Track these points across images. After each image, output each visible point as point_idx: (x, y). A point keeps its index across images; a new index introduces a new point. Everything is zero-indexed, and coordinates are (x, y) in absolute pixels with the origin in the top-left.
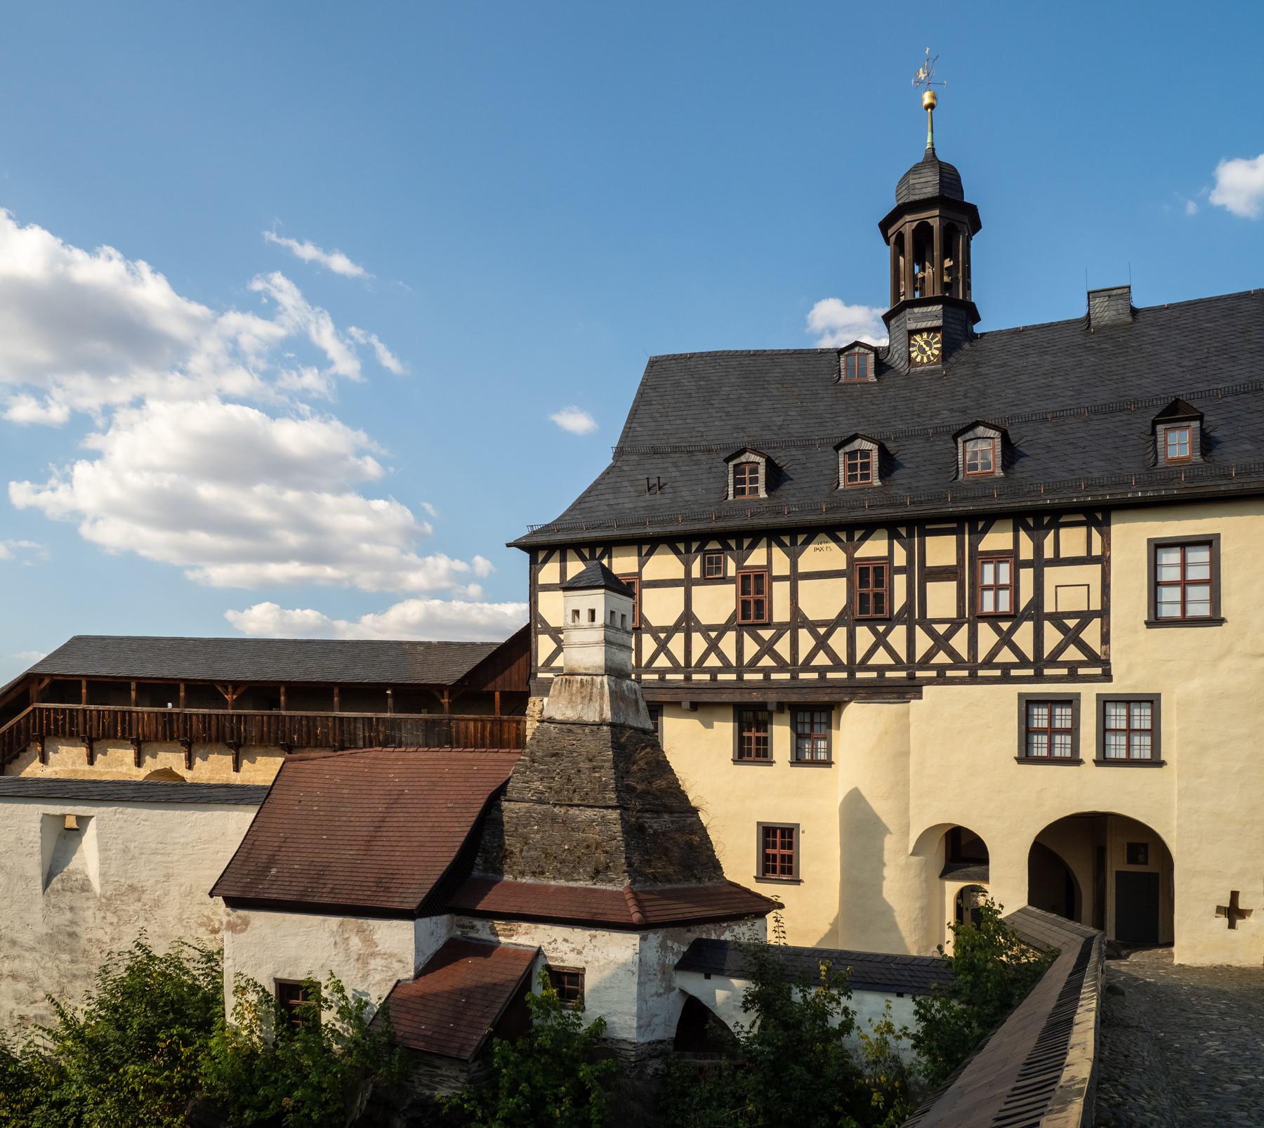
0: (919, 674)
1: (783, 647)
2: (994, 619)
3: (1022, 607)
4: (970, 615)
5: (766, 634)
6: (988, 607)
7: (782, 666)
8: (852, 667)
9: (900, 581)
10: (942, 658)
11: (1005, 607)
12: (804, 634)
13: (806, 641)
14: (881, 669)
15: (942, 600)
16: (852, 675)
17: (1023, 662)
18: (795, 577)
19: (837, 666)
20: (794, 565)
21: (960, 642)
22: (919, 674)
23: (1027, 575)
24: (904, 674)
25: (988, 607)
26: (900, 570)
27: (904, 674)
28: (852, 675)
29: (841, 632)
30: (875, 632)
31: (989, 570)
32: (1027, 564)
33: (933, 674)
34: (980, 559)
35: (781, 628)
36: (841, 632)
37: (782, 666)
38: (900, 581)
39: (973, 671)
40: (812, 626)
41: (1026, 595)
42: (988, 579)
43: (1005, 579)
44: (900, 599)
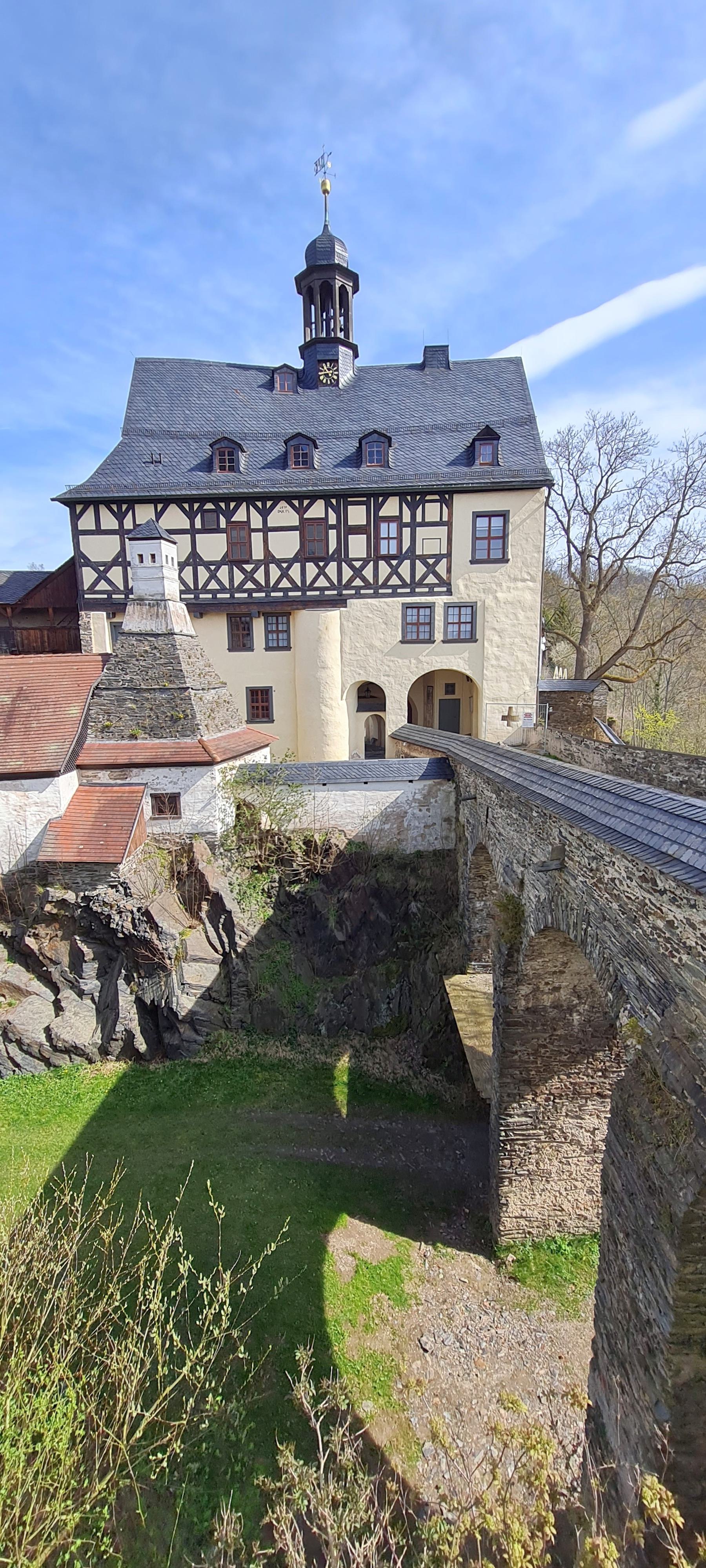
0: (344, 592)
1: (260, 576)
2: (388, 558)
3: (404, 551)
4: (375, 556)
5: (248, 567)
6: (383, 551)
8: (304, 588)
9: (333, 534)
10: (358, 582)
11: (393, 551)
12: (273, 567)
13: (275, 572)
15: (358, 546)
16: (304, 594)
17: (404, 585)
18: (266, 530)
19: (295, 588)
20: (265, 522)
21: (368, 572)
22: (344, 592)
23: (406, 531)
24: (335, 592)
25: (383, 551)
26: (332, 527)
27: (335, 592)
28: (304, 594)
29: (297, 566)
30: (318, 566)
31: (384, 526)
32: (407, 525)
33: (353, 592)
34: (379, 520)
36: (297, 566)
37: (259, 589)
38: (333, 534)
39: (376, 589)
40: (278, 562)
41: (406, 545)
42: (384, 534)
43: (394, 534)
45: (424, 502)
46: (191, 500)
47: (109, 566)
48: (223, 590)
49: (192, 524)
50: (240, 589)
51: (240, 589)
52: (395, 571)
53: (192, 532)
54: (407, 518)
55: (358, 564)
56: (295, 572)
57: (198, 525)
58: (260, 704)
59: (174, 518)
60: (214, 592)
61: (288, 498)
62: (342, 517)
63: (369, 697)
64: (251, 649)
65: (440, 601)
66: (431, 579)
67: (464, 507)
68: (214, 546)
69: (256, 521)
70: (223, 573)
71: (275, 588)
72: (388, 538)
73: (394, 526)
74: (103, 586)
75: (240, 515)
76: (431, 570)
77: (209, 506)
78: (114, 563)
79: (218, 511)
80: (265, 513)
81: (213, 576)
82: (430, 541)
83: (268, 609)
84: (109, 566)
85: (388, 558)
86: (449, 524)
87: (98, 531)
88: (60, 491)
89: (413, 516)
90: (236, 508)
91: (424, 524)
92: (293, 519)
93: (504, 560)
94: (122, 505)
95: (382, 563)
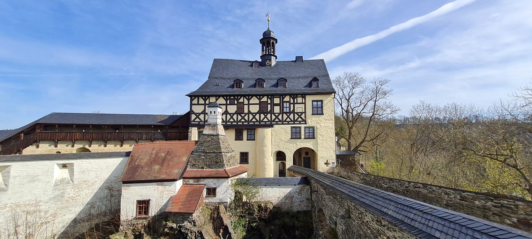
1: (246, 118)
2: (286, 113)
4: (282, 112)
5: (243, 115)
6: (285, 111)
7: (246, 121)
8: (260, 121)
9: (269, 106)
10: (277, 120)
11: (288, 111)
12: (250, 115)
13: (251, 117)
14: (266, 122)
15: (277, 109)
17: (291, 121)
18: (249, 104)
19: (257, 121)
20: (249, 102)
21: (280, 117)
23: (292, 105)
25: (285, 111)
26: (269, 104)
29: (258, 115)
31: (285, 104)
32: (292, 104)
34: (283, 102)
35: (246, 114)
36: (258, 115)
38: (269, 106)
39: (283, 122)
40: (252, 114)
42: (285, 106)
43: (288, 106)
44: (269, 109)
45: (297, 97)
46: (227, 96)
47: (200, 114)
48: (235, 121)
49: (227, 102)
50: (240, 121)
51: (240, 121)
52: (288, 117)
53: (226, 105)
54: (292, 101)
55: (277, 115)
56: (257, 117)
57: (228, 102)
58: (244, 157)
59: (221, 101)
60: (232, 122)
61: (256, 96)
62: (272, 101)
63: (280, 156)
64: (242, 140)
65: (303, 126)
66: (300, 119)
67: (309, 99)
68: (232, 109)
69: (246, 102)
70: (235, 117)
71: (251, 121)
72: (286, 107)
73: (288, 104)
74: (197, 120)
75: (241, 100)
76: (300, 117)
77: (232, 97)
78: (202, 113)
79: (235, 99)
80: (249, 100)
81: (232, 117)
82: (299, 108)
83: (248, 128)
84: (200, 114)
85: (286, 113)
86: (305, 103)
87: (198, 104)
88: (189, 93)
89: (294, 101)
90: (240, 98)
91: (297, 103)
92: (257, 101)
93: (322, 114)
94: (206, 97)
95: (284, 115)
